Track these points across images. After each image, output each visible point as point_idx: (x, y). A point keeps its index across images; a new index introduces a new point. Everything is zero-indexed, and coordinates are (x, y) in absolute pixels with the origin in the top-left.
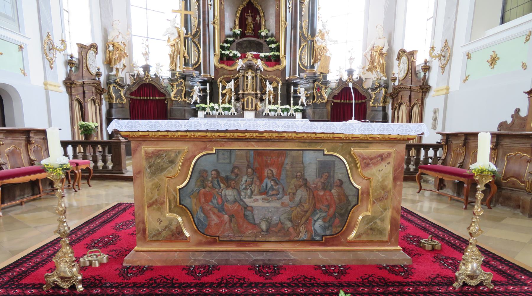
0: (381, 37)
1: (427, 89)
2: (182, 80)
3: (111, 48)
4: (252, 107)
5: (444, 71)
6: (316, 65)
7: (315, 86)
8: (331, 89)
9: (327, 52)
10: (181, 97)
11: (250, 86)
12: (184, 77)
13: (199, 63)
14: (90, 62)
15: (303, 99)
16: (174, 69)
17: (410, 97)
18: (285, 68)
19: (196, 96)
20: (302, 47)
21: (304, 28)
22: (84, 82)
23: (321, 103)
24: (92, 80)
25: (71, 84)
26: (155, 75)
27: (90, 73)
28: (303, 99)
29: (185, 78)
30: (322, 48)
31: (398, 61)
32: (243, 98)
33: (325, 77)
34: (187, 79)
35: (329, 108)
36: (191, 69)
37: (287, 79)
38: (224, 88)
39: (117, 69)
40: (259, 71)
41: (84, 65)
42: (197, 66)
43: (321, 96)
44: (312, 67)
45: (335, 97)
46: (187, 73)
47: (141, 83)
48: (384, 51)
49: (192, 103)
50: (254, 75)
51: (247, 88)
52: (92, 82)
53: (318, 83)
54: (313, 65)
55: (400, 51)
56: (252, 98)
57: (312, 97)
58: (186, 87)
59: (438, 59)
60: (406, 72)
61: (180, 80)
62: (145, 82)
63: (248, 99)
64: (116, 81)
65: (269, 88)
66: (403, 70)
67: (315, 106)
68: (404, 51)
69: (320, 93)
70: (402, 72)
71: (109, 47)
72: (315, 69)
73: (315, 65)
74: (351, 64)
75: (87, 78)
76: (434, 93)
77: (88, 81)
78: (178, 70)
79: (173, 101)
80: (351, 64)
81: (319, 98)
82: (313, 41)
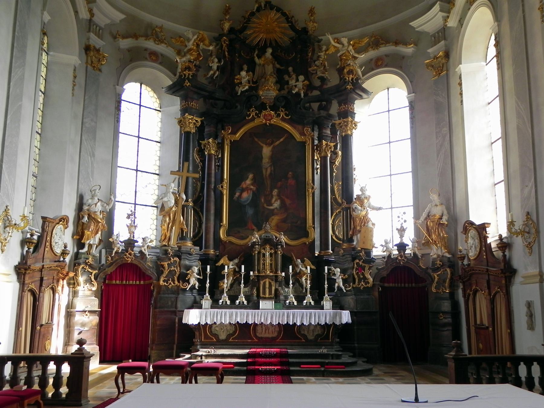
0: (438, 204)
1: (511, 273)
2: (177, 259)
3: (86, 218)
4: (270, 293)
5: (532, 251)
6: (355, 238)
7: (355, 266)
8: (377, 269)
9: (368, 222)
10: (173, 281)
12: (179, 254)
13: (200, 235)
14: (56, 238)
15: (340, 282)
16: (167, 244)
17: (488, 282)
18: (314, 241)
19: (194, 279)
20: (334, 215)
21: (336, 192)
22: (43, 266)
23: (364, 288)
24: (55, 262)
25: (26, 269)
27: (54, 253)
28: (340, 282)
29: (181, 256)
30: (363, 218)
31: (465, 234)
34: (182, 257)
35: (377, 294)
36: (189, 244)
37: (316, 255)
40: (280, 247)
41: (47, 244)
42: (197, 238)
43: (365, 278)
44: (351, 240)
45: (383, 280)
46: (184, 250)
47: (120, 263)
48: (444, 221)
49: (188, 289)
50: (273, 251)
51: (264, 268)
52: (55, 265)
53: (360, 261)
54: (352, 238)
55: (466, 222)
56: (271, 281)
57: (351, 279)
58: (182, 268)
59: (520, 236)
60: (478, 249)
61: (173, 259)
62: (126, 262)
63: (265, 283)
64: (87, 261)
66: (473, 246)
67: (357, 291)
68: (472, 224)
69: (363, 274)
70: (473, 249)
71: (83, 217)
72: (355, 243)
73: (354, 239)
74: (402, 236)
75: (48, 260)
76: (522, 279)
77: (49, 265)
80: (402, 236)
81: (361, 281)
82: (349, 208)
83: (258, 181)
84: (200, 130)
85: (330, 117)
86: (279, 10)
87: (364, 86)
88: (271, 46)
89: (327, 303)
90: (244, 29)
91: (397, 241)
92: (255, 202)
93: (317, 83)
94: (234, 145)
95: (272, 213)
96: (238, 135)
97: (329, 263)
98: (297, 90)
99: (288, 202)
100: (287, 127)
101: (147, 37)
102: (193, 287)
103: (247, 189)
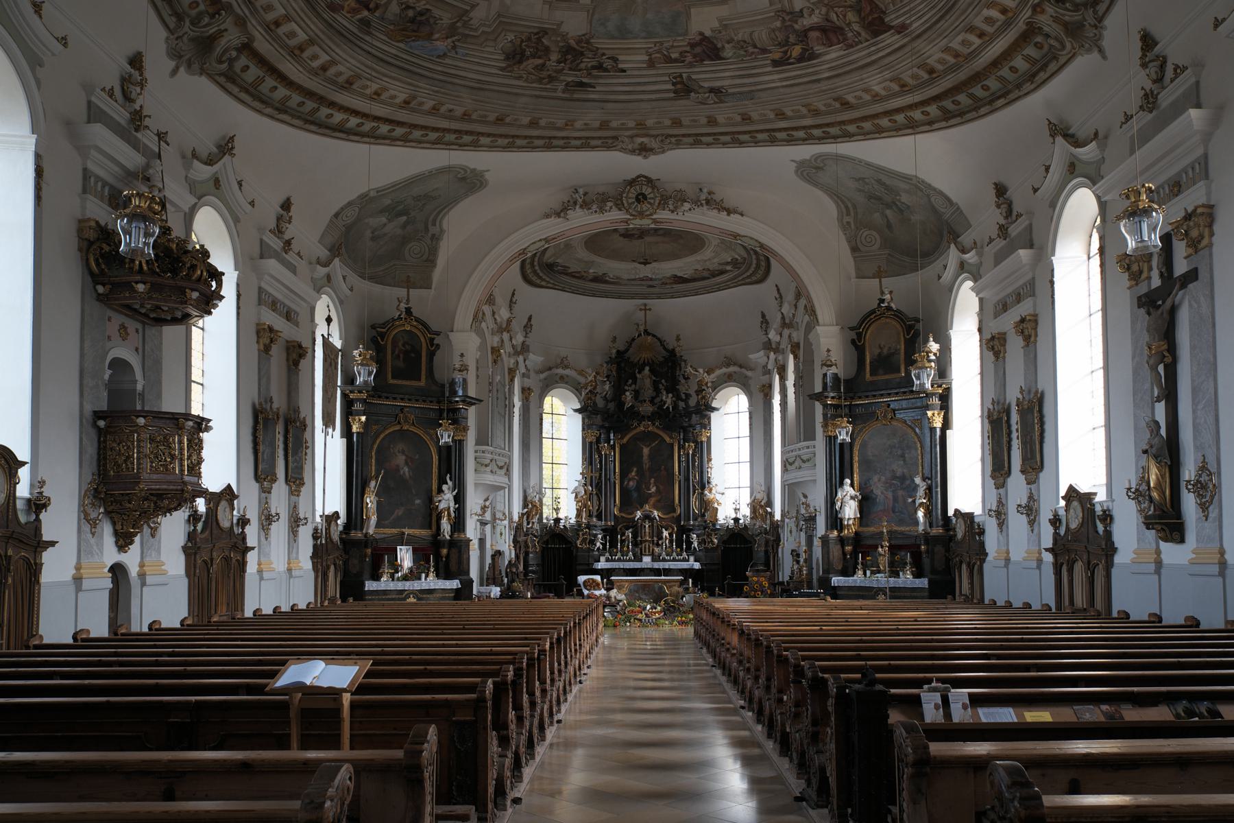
11: (647, 534)
12: (589, 526)
15: (696, 544)
26: (564, 526)
28: (696, 544)
32: (641, 544)
33: (714, 525)
36: (595, 519)
38: (623, 534)
39: (533, 523)
43: (712, 541)
44: (703, 515)
45: (724, 542)
48: (762, 503)
51: (645, 535)
65: (665, 534)
78: (584, 520)
79: (578, 548)
80: (736, 513)
83: (640, 473)
84: (598, 441)
85: (691, 426)
86: (654, 336)
87: (713, 405)
88: (648, 364)
89: (692, 558)
90: (627, 350)
91: (734, 516)
92: (638, 488)
93: (683, 396)
94: (622, 447)
95: (650, 495)
96: (625, 440)
98: (666, 405)
99: (661, 487)
100: (661, 433)
102: (599, 548)
103: (633, 479)
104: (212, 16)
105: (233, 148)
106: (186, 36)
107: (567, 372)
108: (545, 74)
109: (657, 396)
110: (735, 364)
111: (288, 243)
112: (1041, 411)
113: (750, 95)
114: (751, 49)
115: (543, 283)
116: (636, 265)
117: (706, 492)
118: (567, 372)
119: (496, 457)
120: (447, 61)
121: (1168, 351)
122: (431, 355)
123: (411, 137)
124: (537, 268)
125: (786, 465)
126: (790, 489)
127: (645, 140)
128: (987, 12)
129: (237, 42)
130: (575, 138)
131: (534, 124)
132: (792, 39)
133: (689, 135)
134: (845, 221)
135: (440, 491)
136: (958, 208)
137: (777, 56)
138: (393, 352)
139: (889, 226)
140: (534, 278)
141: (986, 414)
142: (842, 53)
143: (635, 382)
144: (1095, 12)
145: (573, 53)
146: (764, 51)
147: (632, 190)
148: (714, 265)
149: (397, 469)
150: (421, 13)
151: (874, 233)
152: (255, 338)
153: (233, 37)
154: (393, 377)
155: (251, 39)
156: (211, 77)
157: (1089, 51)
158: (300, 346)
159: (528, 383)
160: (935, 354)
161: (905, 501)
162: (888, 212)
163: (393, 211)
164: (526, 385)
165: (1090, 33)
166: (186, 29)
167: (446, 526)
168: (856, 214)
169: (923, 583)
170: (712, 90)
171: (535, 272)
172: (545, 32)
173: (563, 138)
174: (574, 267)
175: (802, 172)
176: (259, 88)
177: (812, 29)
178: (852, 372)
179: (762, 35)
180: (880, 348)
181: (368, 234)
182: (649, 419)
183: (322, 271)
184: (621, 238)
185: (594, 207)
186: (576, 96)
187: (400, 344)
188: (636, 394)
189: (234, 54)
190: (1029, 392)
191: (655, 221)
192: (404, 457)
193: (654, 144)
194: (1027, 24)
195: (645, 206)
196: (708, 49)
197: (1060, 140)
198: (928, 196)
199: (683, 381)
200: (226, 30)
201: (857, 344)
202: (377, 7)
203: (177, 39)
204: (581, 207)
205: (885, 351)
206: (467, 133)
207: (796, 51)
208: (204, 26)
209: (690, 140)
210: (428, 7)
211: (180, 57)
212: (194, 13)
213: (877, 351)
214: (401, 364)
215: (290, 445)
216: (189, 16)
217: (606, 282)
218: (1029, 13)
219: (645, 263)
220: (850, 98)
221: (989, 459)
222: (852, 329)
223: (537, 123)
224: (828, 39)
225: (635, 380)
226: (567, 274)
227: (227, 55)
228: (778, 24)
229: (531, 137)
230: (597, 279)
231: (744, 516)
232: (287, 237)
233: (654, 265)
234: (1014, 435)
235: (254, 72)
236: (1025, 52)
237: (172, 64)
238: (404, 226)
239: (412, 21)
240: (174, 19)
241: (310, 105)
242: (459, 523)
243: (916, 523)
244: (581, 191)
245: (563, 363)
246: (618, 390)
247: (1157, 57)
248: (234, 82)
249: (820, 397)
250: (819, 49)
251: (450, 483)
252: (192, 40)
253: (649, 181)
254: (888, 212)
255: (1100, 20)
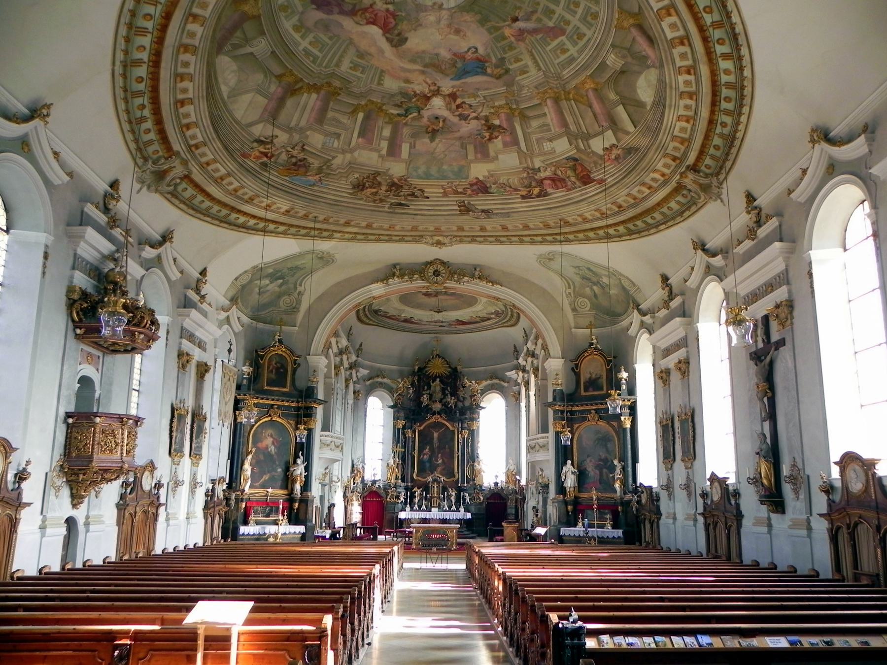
12: (395, 486)
15: (468, 500)
28: (468, 500)
36: (400, 481)
45: (488, 499)
83: (432, 450)
84: (404, 427)
87: (481, 405)
90: (425, 367)
97: (464, 490)
99: (446, 460)
101: (378, 376)
103: (426, 454)
104: (166, 159)
105: (172, 237)
106: (148, 171)
107: (385, 380)
108: (377, 197)
109: (444, 398)
110: (497, 378)
111: (203, 297)
112: (693, 421)
113: (507, 215)
114: (508, 189)
115: (371, 322)
116: (432, 313)
117: (476, 464)
118: (385, 380)
119: (334, 439)
120: (315, 188)
121: (770, 389)
122: (294, 371)
123: (289, 232)
124: (367, 312)
125: (530, 449)
126: (532, 466)
127: (440, 238)
128: (652, 175)
129: (181, 175)
130: (396, 236)
131: (369, 226)
132: (534, 184)
133: (468, 236)
134: (567, 292)
135: (295, 462)
136: (639, 288)
137: (524, 193)
138: (268, 368)
139: (595, 296)
140: (365, 319)
141: (658, 421)
142: (564, 193)
143: (429, 388)
144: (718, 179)
145: (395, 186)
146: (516, 190)
147: (431, 268)
148: (483, 314)
149: (267, 448)
150: (300, 161)
151: (586, 300)
152: (177, 360)
153: (179, 171)
154: (268, 385)
155: (190, 172)
156: (162, 194)
157: (715, 200)
158: (206, 365)
159: (358, 387)
160: (625, 380)
161: (607, 476)
162: (595, 288)
163: (273, 277)
164: (357, 389)
165: (715, 191)
166: (149, 166)
167: (298, 487)
168: (575, 287)
169: (619, 533)
170: (483, 211)
171: (366, 315)
172: (379, 174)
173: (388, 235)
174: (392, 312)
175: (540, 262)
176: (193, 202)
177: (545, 179)
178: (573, 387)
179: (515, 181)
180: (590, 374)
181: (257, 290)
182: (439, 413)
183: (223, 315)
184: (423, 296)
185: (406, 278)
186: (396, 211)
187: (273, 363)
188: (431, 396)
189: (178, 181)
190: (685, 407)
191: (445, 288)
192: (272, 439)
193: (446, 240)
194: (678, 183)
195: (439, 278)
196: (482, 188)
197: (699, 252)
198: (620, 279)
199: (462, 389)
200: (175, 167)
201: (575, 371)
202: (272, 156)
203: (143, 172)
204: (398, 277)
205: (594, 376)
206: (325, 230)
207: (536, 191)
208: (162, 164)
209: (469, 239)
210: (305, 157)
211: (143, 183)
212: (155, 157)
213: (588, 376)
214: (273, 376)
215: (195, 431)
216: (151, 159)
217: (412, 323)
218: (678, 177)
219: (438, 312)
220: (570, 219)
221: (661, 450)
222: (572, 361)
223: (371, 226)
224: (555, 184)
225: (429, 388)
226: (386, 317)
227: (174, 182)
228: (525, 175)
229: (367, 234)
230: (406, 321)
231: (502, 482)
232: (202, 293)
233: (444, 313)
234: (677, 435)
235: (190, 192)
236: (676, 199)
237: (139, 186)
238: (280, 286)
239: (295, 164)
240: (142, 160)
241: (224, 212)
242: (306, 486)
243: (615, 491)
244: (398, 267)
245: (380, 373)
246: (418, 394)
247: (756, 208)
248: (177, 198)
249: (550, 405)
250: (550, 190)
251: (302, 457)
252: (152, 172)
253: (443, 263)
254: (595, 288)
255: (721, 184)
